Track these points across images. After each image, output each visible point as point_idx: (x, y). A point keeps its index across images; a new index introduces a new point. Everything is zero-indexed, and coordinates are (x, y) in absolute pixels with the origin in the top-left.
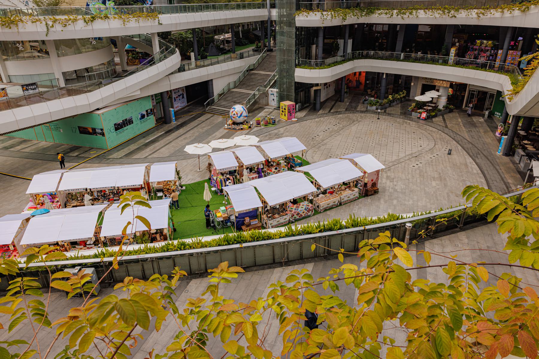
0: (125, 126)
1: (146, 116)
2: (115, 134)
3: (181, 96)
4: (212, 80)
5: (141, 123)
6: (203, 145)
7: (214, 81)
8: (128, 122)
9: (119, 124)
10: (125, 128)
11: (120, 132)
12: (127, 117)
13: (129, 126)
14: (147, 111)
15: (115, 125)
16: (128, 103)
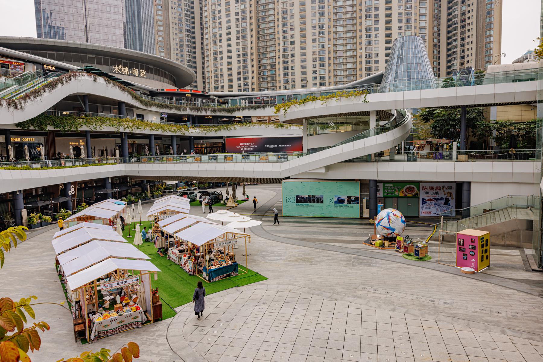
0: (310, 202)
1: (346, 202)
2: (295, 204)
3: (444, 201)
4: (469, 183)
5: (336, 207)
6: (239, 215)
7: (472, 185)
8: (311, 199)
9: (303, 198)
10: (310, 204)
11: (302, 206)
12: (317, 194)
13: (316, 204)
14: (349, 197)
15: (297, 196)
16: (320, 181)
